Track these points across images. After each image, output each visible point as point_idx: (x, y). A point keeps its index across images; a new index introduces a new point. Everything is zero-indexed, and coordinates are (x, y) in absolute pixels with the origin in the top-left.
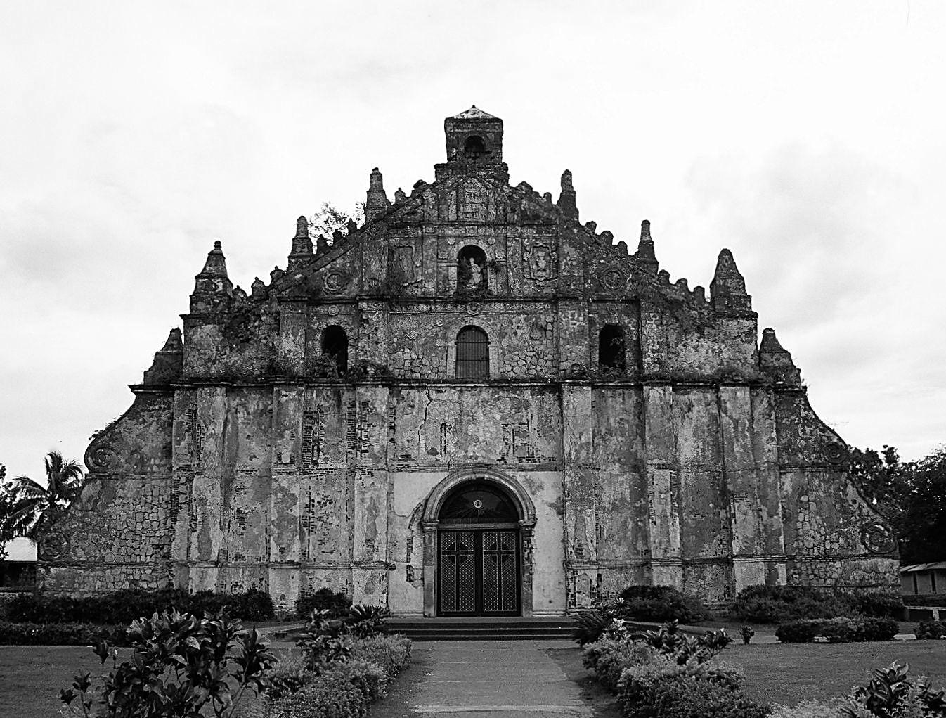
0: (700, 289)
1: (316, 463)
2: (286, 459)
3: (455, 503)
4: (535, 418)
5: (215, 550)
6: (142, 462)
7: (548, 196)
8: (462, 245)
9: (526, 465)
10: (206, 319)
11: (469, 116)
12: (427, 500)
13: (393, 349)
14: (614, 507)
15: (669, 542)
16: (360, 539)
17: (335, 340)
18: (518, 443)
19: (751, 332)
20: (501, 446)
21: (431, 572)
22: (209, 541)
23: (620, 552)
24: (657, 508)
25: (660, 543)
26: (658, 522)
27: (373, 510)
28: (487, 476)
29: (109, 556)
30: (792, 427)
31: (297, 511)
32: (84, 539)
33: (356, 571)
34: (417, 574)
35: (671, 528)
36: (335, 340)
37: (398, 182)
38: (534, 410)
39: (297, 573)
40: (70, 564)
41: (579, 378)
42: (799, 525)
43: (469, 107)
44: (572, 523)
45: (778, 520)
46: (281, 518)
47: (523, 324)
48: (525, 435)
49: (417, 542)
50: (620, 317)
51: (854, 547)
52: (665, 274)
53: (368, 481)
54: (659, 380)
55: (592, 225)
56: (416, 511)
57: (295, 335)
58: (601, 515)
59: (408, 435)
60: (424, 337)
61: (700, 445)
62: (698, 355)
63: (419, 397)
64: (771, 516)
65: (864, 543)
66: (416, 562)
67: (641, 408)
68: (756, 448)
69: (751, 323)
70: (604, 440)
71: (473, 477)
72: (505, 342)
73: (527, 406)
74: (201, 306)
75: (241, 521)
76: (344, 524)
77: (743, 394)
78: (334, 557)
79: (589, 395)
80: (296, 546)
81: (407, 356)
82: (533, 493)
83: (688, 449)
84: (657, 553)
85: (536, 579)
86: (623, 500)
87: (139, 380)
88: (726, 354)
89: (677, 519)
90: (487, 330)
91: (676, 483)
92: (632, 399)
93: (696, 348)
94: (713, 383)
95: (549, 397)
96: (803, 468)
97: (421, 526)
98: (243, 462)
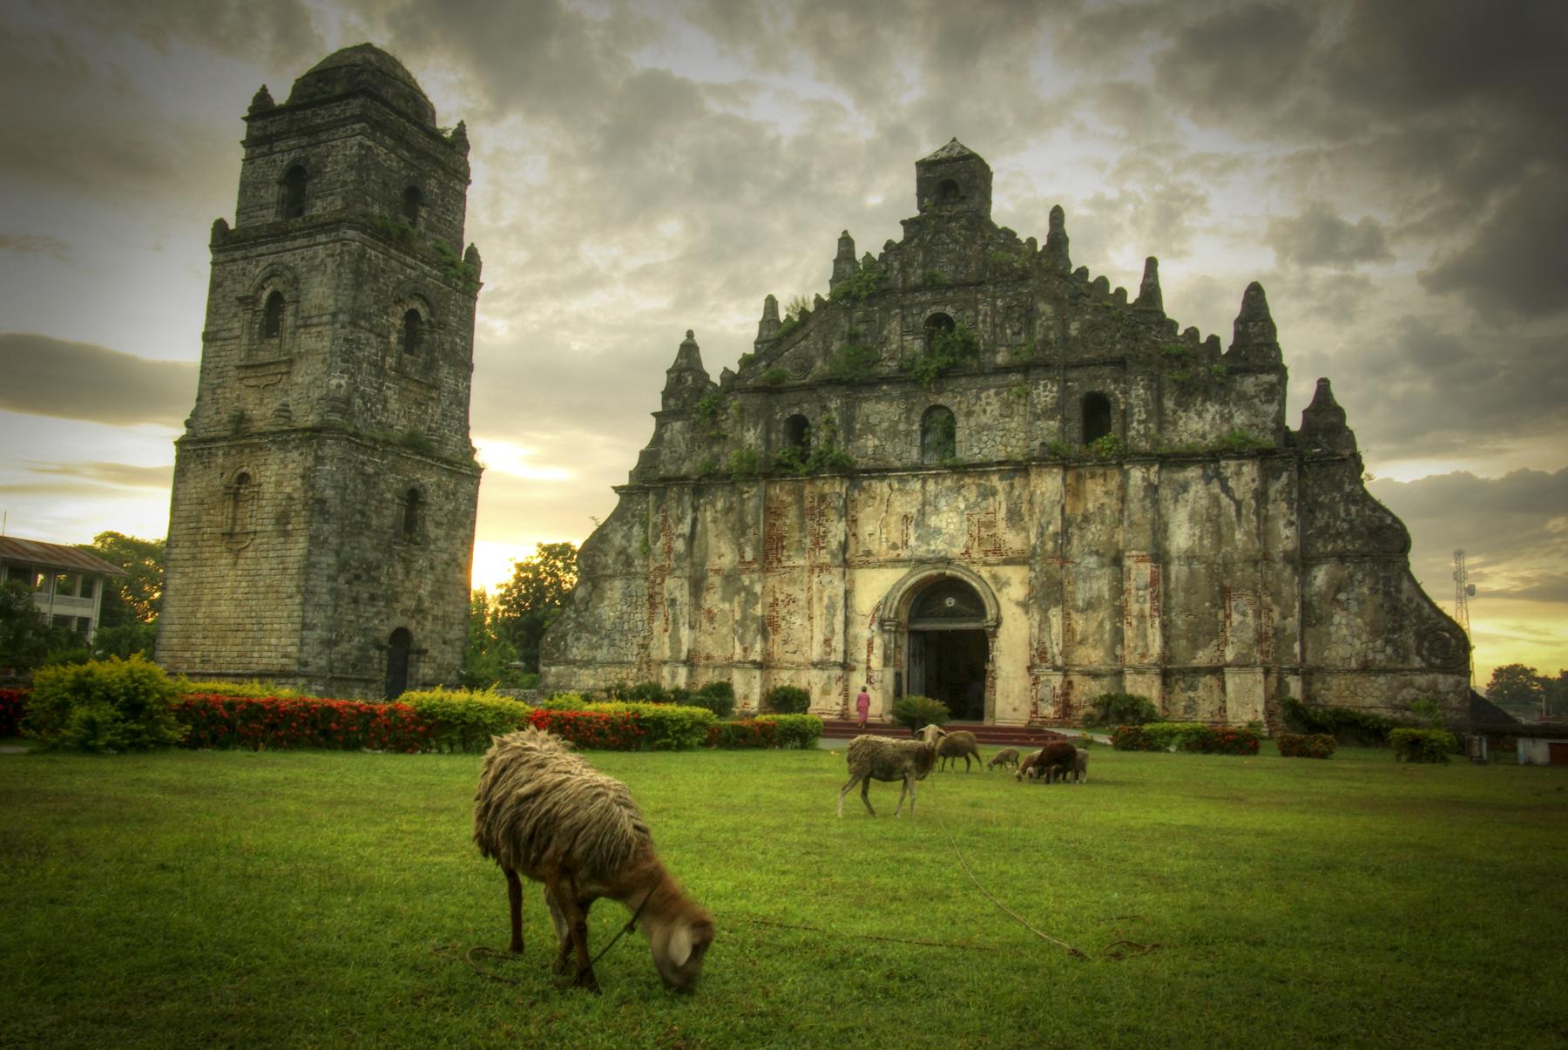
0: (1214, 341)
1: (780, 561)
2: (749, 556)
4: (1004, 507)
5: (685, 649)
6: (629, 562)
7: (1032, 242)
8: (929, 313)
9: (991, 559)
11: (944, 154)
12: (887, 598)
14: (1090, 606)
15: (1146, 646)
16: (819, 638)
18: (984, 534)
19: (1277, 392)
20: (965, 538)
21: (889, 675)
22: (679, 641)
24: (1134, 608)
25: (1136, 648)
26: (1134, 623)
27: (831, 608)
28: (948, 572)
29: (601, 655)
30: (1332, 508)
32: (578, 639)
33: (814, 672)
34: (876, 676)
35: (1150, 631)
36: (798, 428)
37: (869, 245)
38: (1001, 497)
39: (757, 673)
40: (568, 663)
42: (1333, 629)
43: (947, 142)
44: (1036, 624)
45: (1293, 623)
46: (744, 618)
47: (993, 400)
48: (991, 525)
49: (878, 642)
50: (1104, 384)
51: (1405, 658)
52: (1173, 325)
53: (826, 578)
54: (1146, 459)
55: (1083, 272)
56: (877, 609)
57: (755, 427)
58: (1074, 615)
59: (869, 529)
60: (884, 423)
61: (1197, 532)
62: (1198, 425)
63: (881, 487)
64: (1284, 618)
65: (1419, 654)
66: (876, 662)
68: (1264, 532)
69: (1273, 378)
70: (1081, 529)
71: (934, 572)
72: (972, 422)
73: (994, 493)
74: (672, 402)
75: (711, 619)
76: (807, 624)
77: (1250, 470)
78: (797, 658)
79: (1059, 479)
80: (758, 647)
81: (870, 443)
82: (999, 590)
83: (1181, 537)
84: (1132, 659)
85: (1000, 684)
86: (1100, 597)
87: (625, 481)
88: (1240, 419)
89: (1157, 621)
90: (954, 409)
91: (1160, 580)
93: (1200, 415)
94: (1210, 458)
95: (1018, 482)
96: (1342, 557)
97: (882, 623)
98: (714, 562)
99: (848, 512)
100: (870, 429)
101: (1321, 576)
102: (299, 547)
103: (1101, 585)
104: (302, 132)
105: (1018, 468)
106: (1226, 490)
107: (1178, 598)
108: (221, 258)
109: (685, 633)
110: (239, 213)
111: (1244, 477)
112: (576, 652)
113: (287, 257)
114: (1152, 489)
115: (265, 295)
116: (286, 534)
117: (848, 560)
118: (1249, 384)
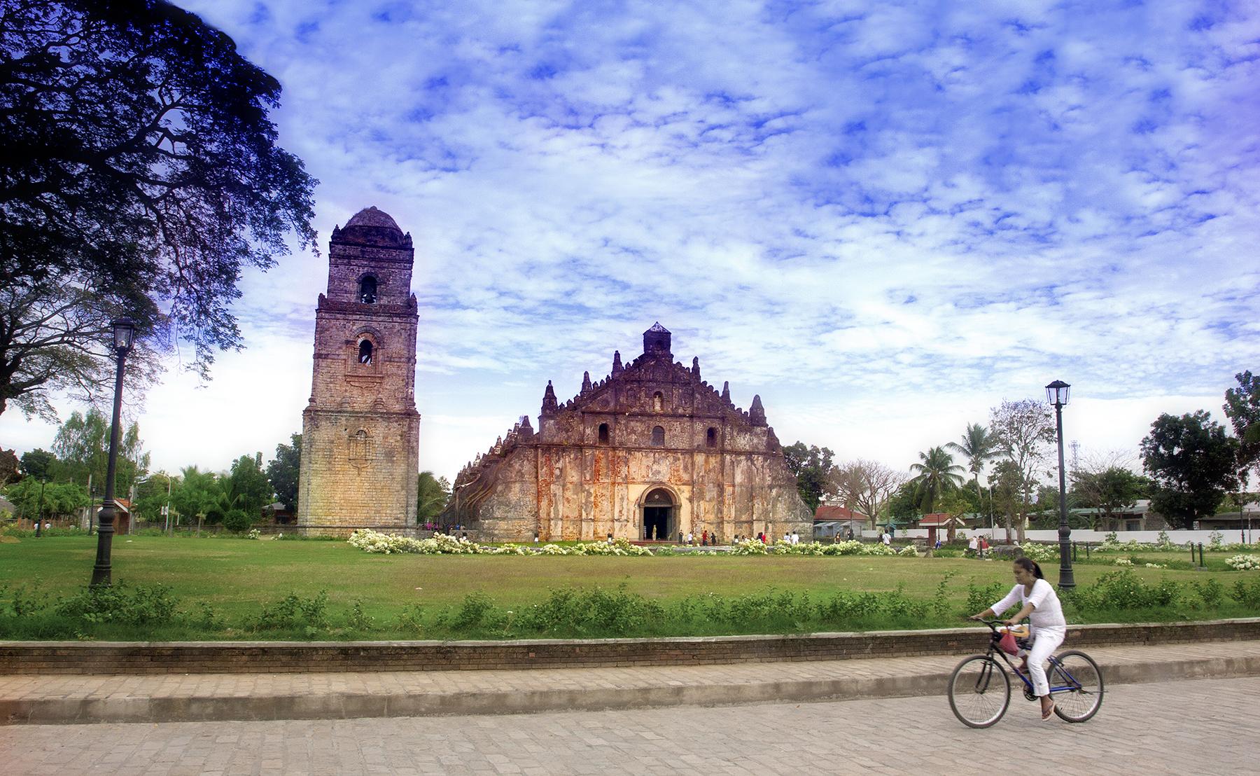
3: (650, 497)
6: (522, 475)
10: (551, 417)
13: (628, 434)
17: (604, 430)
23: (712, 517)
27: (622, 499)
31: (592, 499)
37: (628, 358)
41: (699, 450)
54: (732, 452)
55: (705, 383)
62: (743, 441)
63: (638, 455)
67: (723, 461)
68: (763, 479)
88: (755, 441)
92: (719, 459)
94: (749, 455)
98: (569, 479)
99: (626, 463)
100: (634, 432)
101: (774, 491)
102: (400, 470)
103: (715, 493)
104: (373, 260)
105: (691, 452)
106: (752, 463)
107: (738, 498)
108: (327, 316)
109: (560, 507)
110: (328, 292)
111: (759, 460)
112: (497, 514)
113: (374, 325)
114: (732, 462)
115: (360, 341)
116: (393, 462)
117: (628, 481)
118: (758, 430)
